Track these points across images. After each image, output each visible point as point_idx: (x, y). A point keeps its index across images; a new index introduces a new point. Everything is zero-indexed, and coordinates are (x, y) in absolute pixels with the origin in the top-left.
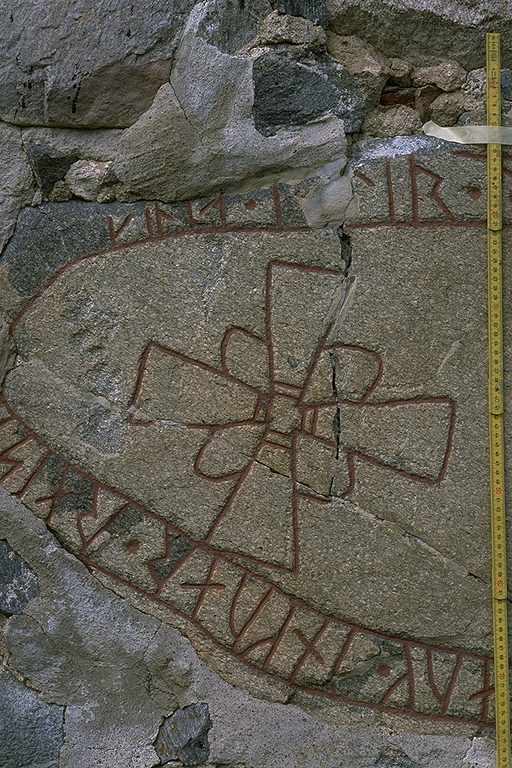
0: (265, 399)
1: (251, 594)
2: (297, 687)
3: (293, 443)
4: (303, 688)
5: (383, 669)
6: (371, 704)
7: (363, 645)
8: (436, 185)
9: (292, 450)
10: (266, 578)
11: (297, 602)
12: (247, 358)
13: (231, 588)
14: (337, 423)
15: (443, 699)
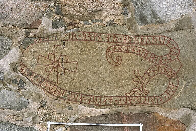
0: (54, 62)
1: (52, 86)
2: (58, 98)
3: (57, 67)
4: (59, 98)
5: (69, 96)
6: (67, 100)
7: (66, 92)
8: (75, 35)
9: (57, 68)
11: (58, 87)
12: (52, 57)
13: (50, 85)
14: (63, 65)
15: (76, 99)
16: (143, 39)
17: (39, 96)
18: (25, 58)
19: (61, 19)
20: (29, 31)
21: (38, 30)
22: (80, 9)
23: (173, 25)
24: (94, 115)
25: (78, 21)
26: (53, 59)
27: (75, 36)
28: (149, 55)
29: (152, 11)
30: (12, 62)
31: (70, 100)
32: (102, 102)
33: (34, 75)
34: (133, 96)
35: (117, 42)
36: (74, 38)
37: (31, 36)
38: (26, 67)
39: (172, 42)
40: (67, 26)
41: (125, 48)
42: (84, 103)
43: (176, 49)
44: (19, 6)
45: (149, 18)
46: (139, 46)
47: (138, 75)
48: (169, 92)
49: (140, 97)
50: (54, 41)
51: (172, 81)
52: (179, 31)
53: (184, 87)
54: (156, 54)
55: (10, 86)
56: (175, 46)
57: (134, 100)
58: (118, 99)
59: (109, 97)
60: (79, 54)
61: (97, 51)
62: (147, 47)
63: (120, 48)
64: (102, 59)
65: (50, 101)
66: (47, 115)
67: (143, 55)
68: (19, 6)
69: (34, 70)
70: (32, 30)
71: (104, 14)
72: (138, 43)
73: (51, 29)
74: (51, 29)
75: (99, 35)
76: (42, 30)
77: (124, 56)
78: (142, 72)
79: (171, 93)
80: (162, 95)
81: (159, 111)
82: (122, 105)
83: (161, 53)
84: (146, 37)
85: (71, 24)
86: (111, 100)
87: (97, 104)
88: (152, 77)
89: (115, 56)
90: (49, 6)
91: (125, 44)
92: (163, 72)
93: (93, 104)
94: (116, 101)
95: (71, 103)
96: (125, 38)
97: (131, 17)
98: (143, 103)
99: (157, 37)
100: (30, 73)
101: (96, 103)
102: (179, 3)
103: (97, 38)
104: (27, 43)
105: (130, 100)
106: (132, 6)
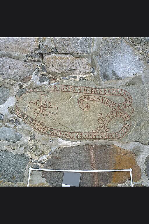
0: (40, 107)
1: (39, 125)
5: (51, 132)
7: (49, 129)
10: (40, 123)
16: (105, 91)
17: (30, 132)
18: (19, 104)
19: (46, 75)
20: (22, 84)
21: (29, 84)
22: (60, 68)
23: (128, 81)
24: (69, 146)
25: (58, 77)
26: (39, 105)
27: (56, 88)
28: (110, 103)
29: (113, 70)
30: (10, 106)
31: (52, 135)
32: (75, 136)
33: (26, 116)
34: (97, 133)
35: (87, 93)
36: (55, 90)
37: (24, 88)
38: (20, 110)
39: (126, 93)
40: (50, 81)
41: (92, 97)
42: (62, 137)
43: (130, 99)
44: (15, 65)
45: (110, 76)
46: (103, 96)
47: (101, 118)
48: (124, 130)
49: (102, 134)
50: (41, 91)
51: (126, 122)
52: (132, 86)
53: (135, 127)
54: (115, 102)
55: (8, 124)
56: (129, 96)
57: (99, 136)
58: (87, 135)
59: (81, 133)
60: (59, 102)
61: (72, 99)
62: (108, 97)
63: (89, 98)
64: (76, 105)
65: (37, 134)
66: (35, 145)
67: (105, 103)
68: (15, 65)
69: (26, 113)
70: (25, 83)
71: (77, 72)
72: (102, 94)
73: (38, 83)
74: (38, 83)
75: (73, 87)
76: (32, 83)
77: (92, 104)
78: (105, 115)
79: (125, 131)
80: (118, 132)
81: (117, 144)
82: (89, 139)
83: (119, 102)
84: (108, 90)
85: (53, 79)
86: (81, 136)
87: (71, 138)
88: (112, 119)
89: (86, 103)
90: (37, 65)
91: (92, 95)
92: (120, 115)
93: (68, 138)
94: (85, 136)
95: (53, 137)
96: (92, 90)
97: (97, 75)
98: (104, 138)
99: (116, 90)
100: (23, 115)
101: (70, 137)
102: (133, 65)
103: (72, 90)
104: (21, 93)
105: (95, 135)
106: (98, 67)
